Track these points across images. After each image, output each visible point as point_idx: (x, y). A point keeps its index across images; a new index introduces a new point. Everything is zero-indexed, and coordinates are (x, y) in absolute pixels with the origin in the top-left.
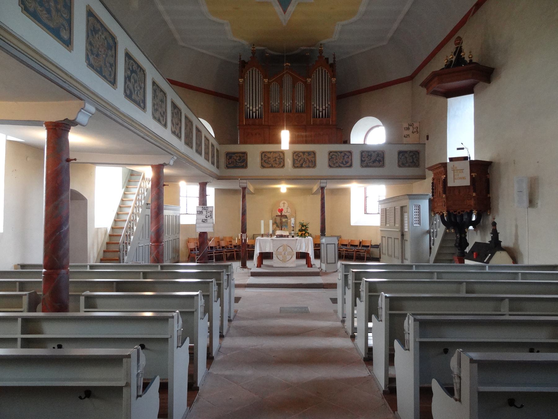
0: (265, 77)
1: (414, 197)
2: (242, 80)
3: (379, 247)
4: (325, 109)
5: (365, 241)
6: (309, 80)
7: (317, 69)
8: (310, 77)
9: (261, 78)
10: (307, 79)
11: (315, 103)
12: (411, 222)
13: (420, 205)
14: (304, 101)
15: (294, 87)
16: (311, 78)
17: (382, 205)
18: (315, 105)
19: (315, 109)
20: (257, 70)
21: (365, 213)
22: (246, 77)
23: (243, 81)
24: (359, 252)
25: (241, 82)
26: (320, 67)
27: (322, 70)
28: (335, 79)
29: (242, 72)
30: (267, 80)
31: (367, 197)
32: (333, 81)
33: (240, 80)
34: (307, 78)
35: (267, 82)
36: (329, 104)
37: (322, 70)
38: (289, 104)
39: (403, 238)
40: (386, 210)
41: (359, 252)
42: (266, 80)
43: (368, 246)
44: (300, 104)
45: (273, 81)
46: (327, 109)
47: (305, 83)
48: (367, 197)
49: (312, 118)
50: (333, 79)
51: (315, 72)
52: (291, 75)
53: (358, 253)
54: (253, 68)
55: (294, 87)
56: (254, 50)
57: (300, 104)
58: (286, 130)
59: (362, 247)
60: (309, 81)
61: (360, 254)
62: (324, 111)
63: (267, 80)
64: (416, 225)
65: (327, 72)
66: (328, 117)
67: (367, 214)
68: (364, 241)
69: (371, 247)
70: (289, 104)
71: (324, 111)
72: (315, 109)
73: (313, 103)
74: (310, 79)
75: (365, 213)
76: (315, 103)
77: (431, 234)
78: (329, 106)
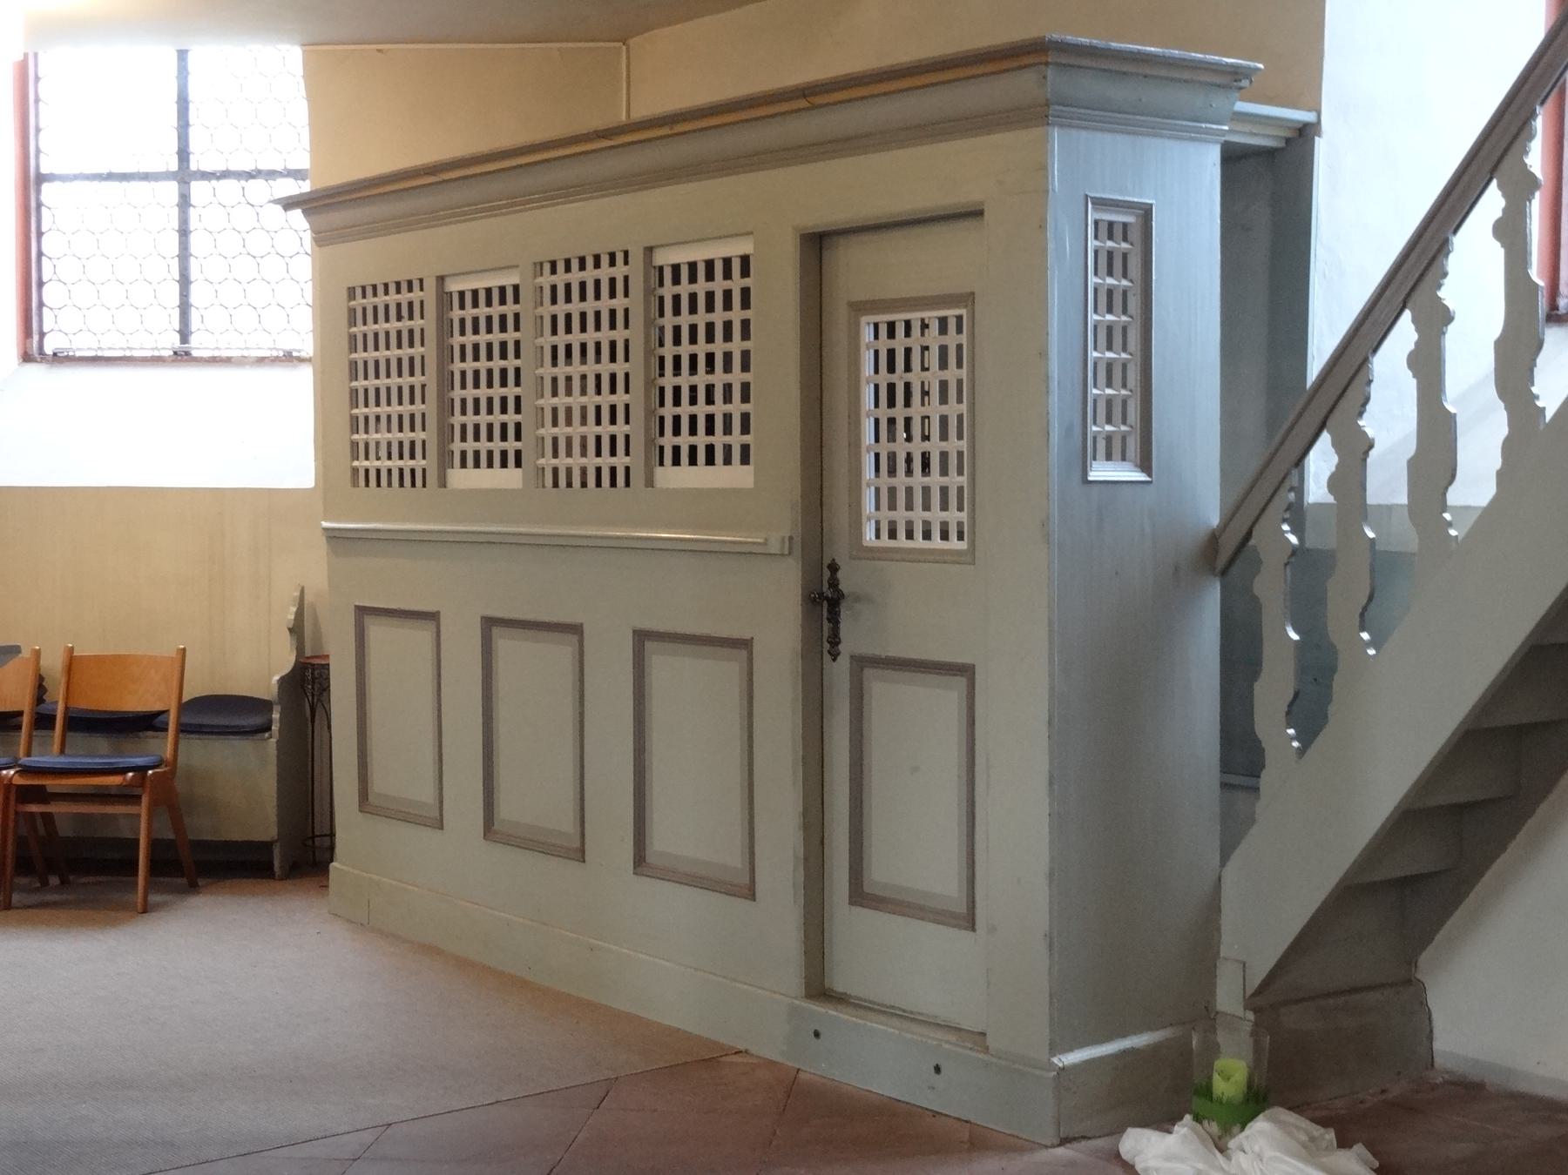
1: (1119, 92)
3: (267, 728)
5: (117, 662)
12: (1068, 431)
13: (1146, 213)
17: (361, 246)
21: (27, 357)
24: (40, 795)
31: (41, 179)
39: (835, 640)
40: (444, 299)
41: (40, 795)
43: (149, 722)
48: (41, 179)
53: (34, 808)
59: (78, 739)
61: (48, 818)
64: (1102, 471)
67: (58, 359)
68: (100, 660)
69: (185, 729)
75: (27, 357)
77: (1270, 587)
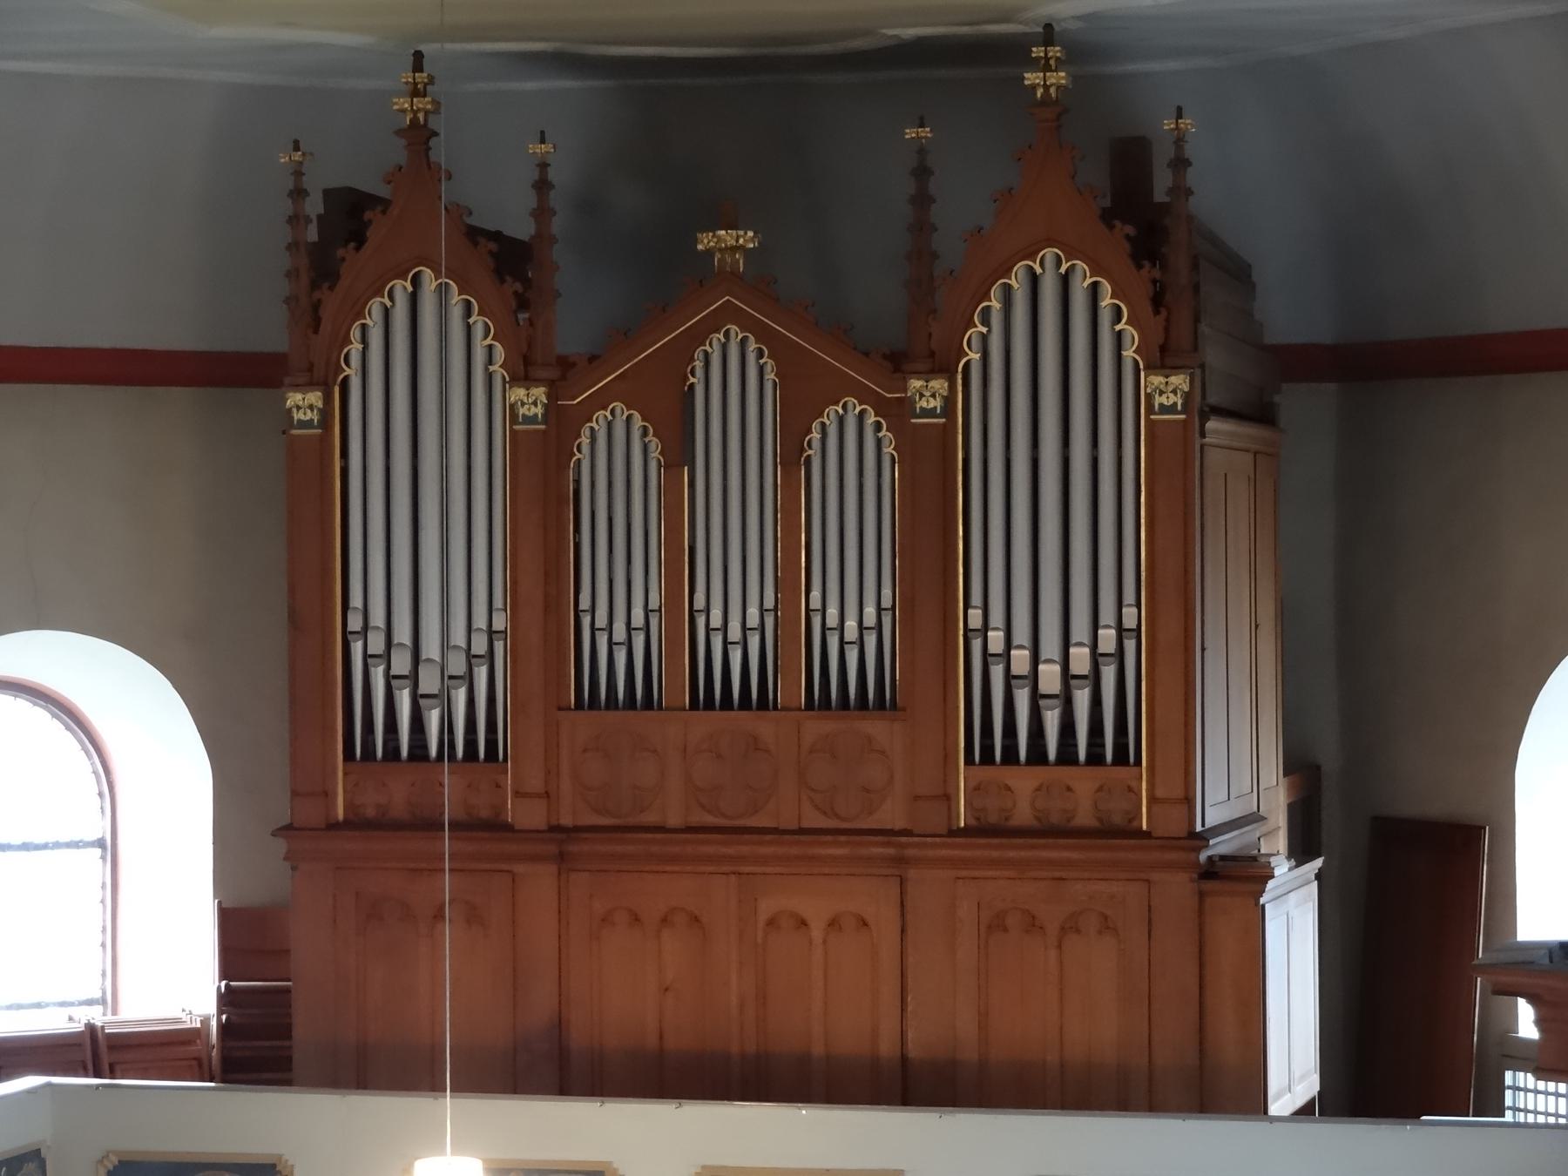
0: (522, 373)
2: (315, 398)
4: (1095, 678)
6: (927, 393)
7: (1017, 281)
8: (943, 364)
9: (489, 377)
10: (916, 384)
11: (997, 617)
14: (887, 592)
15: (792, 456)
16: (947, 371)
18: (996, 639)
19: (997, 672)
20: (456, 298)
22: (352, 372)
23: (325, 414)
25: (298, 416)
26: (1049, 253)
27: (1065, 281)
28: (1179, 381)
29: (316, 332)
30: (540, 392)
32: (1163, 400)
33: (294, 398)
34: (918, 374)
35: (539, 410)
36: (1130, 621)
37: (1065, 281)
38: (753, 620)
42: (531, 400)
44: (851, 624)
45: (600, 401)
46: (1109, 674)
47: (897, 412)
49: (969, 760)
50: (1157, 380)
51: (995, 304)
52: (764, 335)
54: (416, 281)
55: (792, 456)
56: (415, 113)
57: (851, 624)
58: (454, 1153)
60: (935, 403)
62: (1082, 698)
63: (540, 392)
65: (1106, 302)
66: (1121, 757)
70: (753, 620)
71: (1082, 698)
72: (997, 672)
73: (975, 618)
74: (939, 385)
76: (997, 617)
78: (1130, 645)
